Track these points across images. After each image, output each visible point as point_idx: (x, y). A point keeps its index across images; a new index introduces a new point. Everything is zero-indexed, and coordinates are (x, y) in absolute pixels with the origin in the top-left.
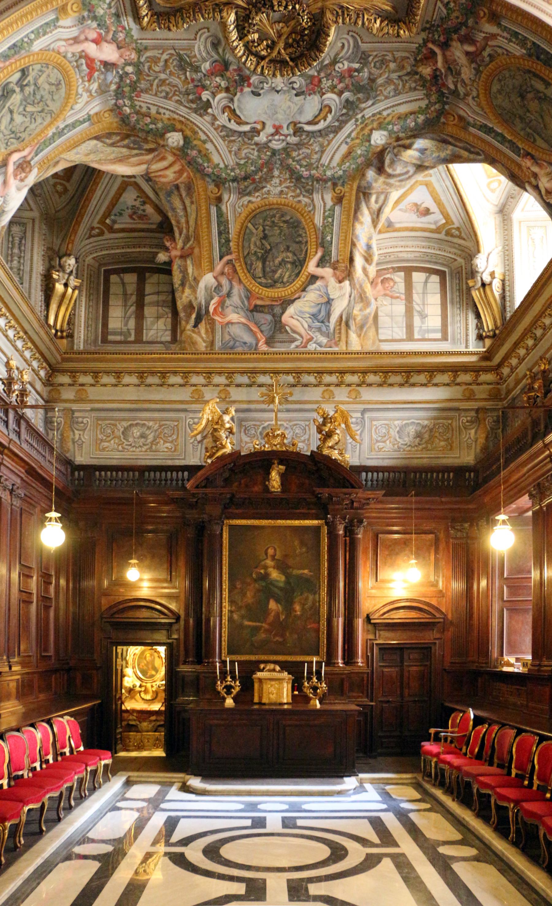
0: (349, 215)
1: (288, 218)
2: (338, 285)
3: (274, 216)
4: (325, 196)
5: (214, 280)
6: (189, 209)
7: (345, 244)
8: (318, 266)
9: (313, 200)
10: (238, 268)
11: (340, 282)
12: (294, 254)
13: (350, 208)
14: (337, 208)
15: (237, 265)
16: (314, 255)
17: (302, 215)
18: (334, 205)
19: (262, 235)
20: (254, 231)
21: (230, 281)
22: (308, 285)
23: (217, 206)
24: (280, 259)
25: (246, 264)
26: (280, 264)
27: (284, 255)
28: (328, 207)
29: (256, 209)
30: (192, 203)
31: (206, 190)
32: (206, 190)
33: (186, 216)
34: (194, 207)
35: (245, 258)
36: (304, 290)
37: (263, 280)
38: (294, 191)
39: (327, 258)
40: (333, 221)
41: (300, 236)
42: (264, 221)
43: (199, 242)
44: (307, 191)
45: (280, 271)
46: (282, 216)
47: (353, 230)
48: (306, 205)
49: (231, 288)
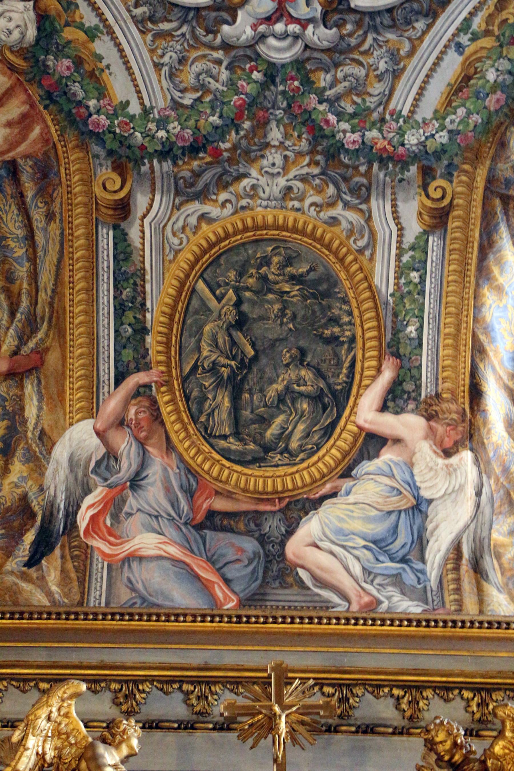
0: (464, 263)
1: (303, 269)
2: (441, 462)
3: (266, 261)
4: (401, 206)
5: (96, 441)
6: (40, 238)
7: (456, 347)
8: (384, 408)
9: (369, 219)
10: (166, 410)
11: (447, 453)
12: (319, 373)
13: (467, 241)
14: (434, 242)
15: (163, 399)
16: (374, 378)
17: (342, 261)
18: (426, 233)
19: (231, 317)
20: (213, 303)
21: (142, 444)
22: (356, 462)
23: (116, 227)
24: (279, 386)
25: (187, 398)
26: (281, 400)
27: (292, 374)
28: (409, 238)
29: (220, 240)
30: (50, 217)
31: (88, 182)
32: (88, 182)
33: (33, 259)
34: (54, 228)
35: (184, 380)
36: (347, 474)
37: (233, 444)
38: (319, 191)
39: (409, 386)
40: (423, 279)
41: (335, 321)
42: (240, 275)
43: (61, 333)
44: (355, 191)
45: (280, 420)
46: (289, 261)
47: (477, 308)
48: (351, 232)
49: (143, 465)
